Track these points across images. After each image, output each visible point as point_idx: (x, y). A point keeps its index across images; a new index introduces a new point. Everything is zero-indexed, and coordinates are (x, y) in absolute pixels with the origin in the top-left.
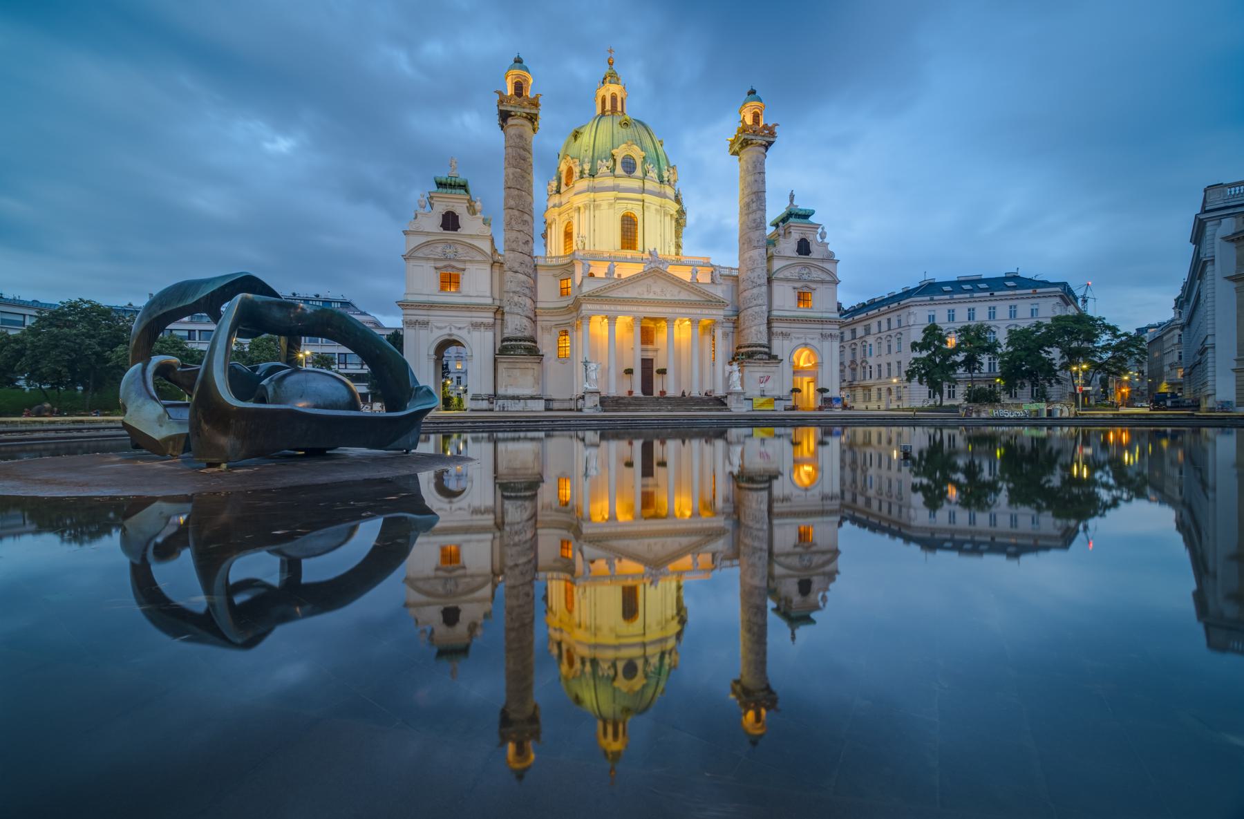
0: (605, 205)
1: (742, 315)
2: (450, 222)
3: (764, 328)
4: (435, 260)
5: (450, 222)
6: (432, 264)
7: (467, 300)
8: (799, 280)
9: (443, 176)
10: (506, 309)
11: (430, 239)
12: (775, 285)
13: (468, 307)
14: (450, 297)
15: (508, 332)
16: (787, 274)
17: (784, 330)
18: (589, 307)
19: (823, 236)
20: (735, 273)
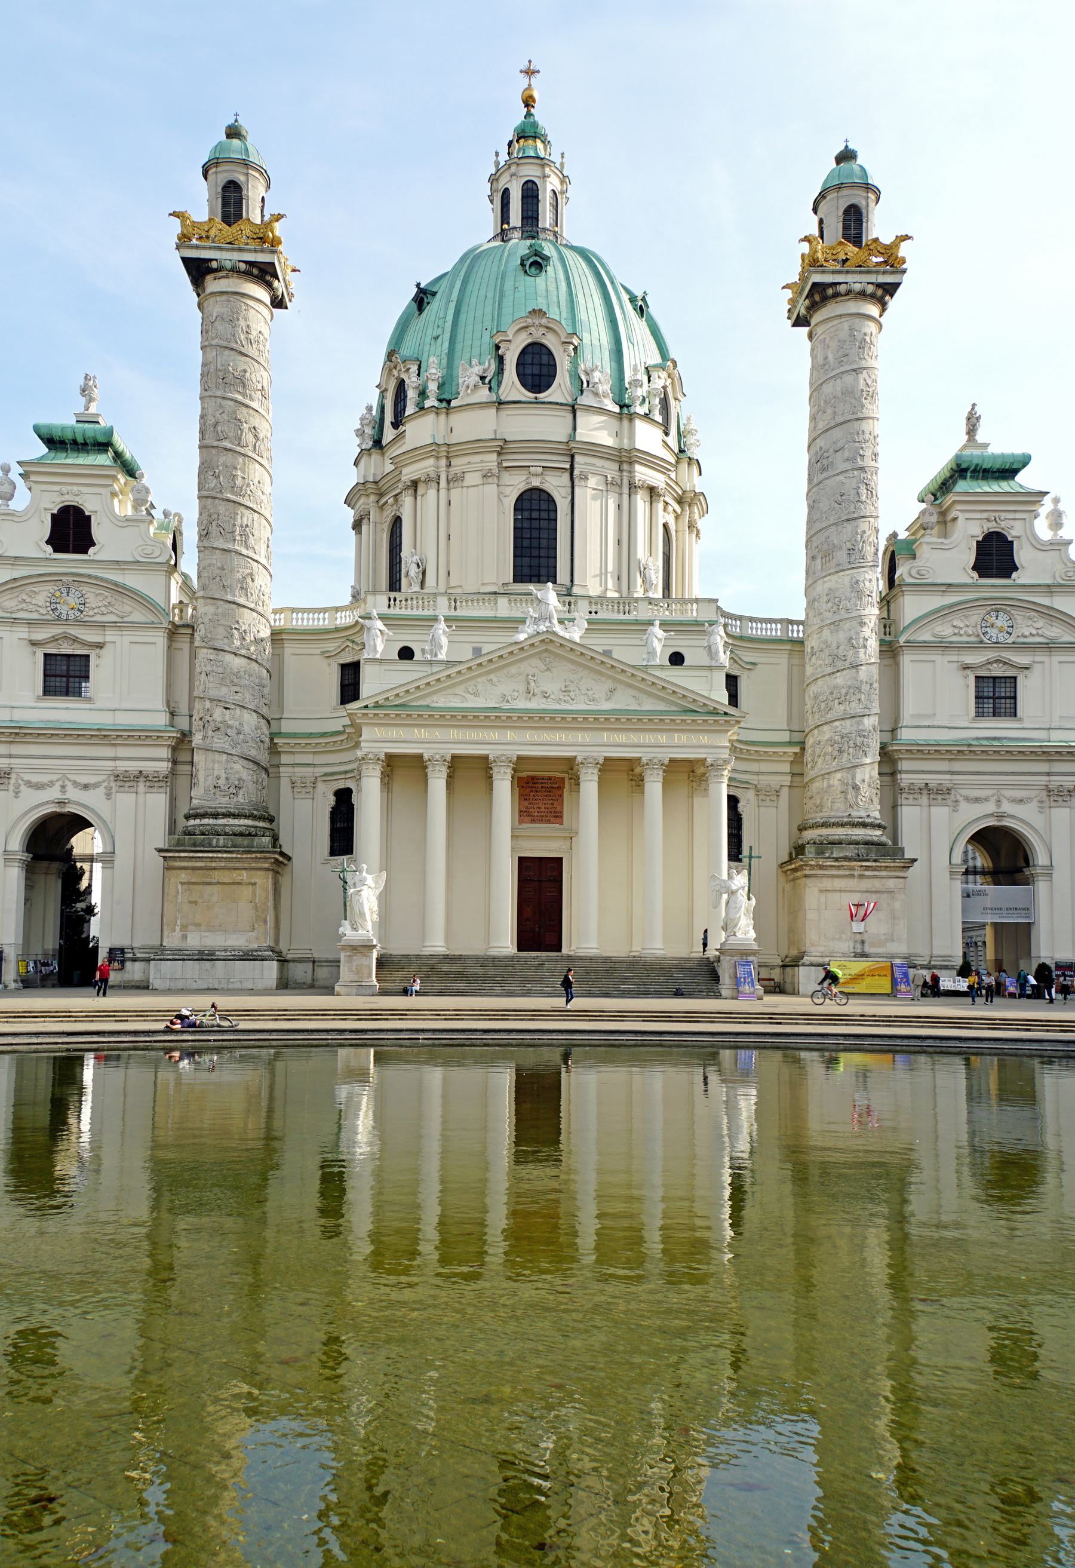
0: (472, 479)
1: (810, 741)
2: (71, 530)
3: (869, 772)
4: (30, 623)
5: (71, 530)
6: (23, 632)
7: (105, 720)
8: (979, 645)
9: (63, 418)
10: (197, 739)
11: (17, 573)
12: (907, 660)
13: (103, 736)
14: (64, 711)
15: (200, 797)
16: (944, 630)
17: (933, 780)
18: (379, 733)
19: (1056, 520)
20: (797, 632)
